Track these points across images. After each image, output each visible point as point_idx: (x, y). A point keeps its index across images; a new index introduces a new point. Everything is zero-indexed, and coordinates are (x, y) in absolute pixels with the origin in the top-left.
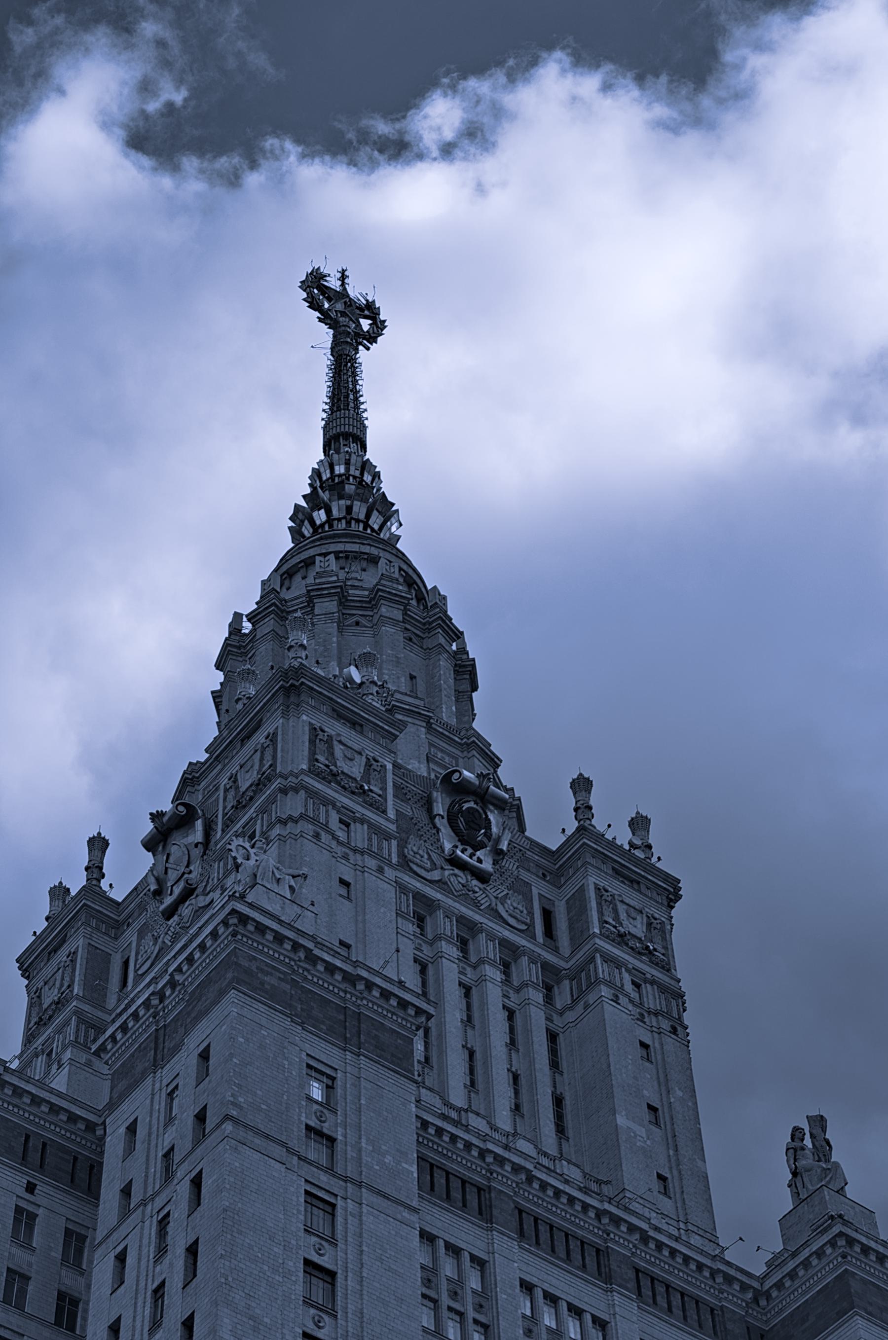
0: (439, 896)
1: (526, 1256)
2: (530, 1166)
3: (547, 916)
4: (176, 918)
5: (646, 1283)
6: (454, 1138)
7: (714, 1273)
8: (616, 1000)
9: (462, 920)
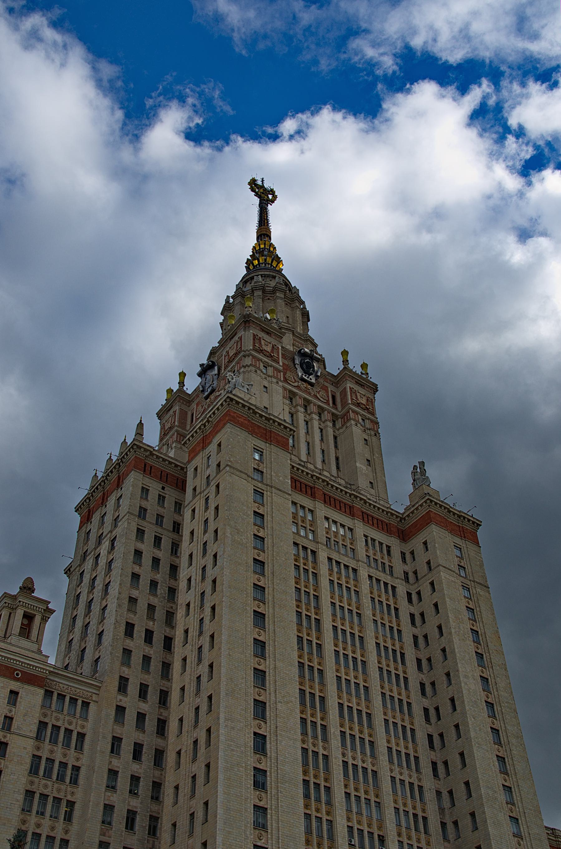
0: (297, 391)
1: (327, 508)
2: (328, 480)
3: (334, 397)
4: (209, 399)
5: (365, 516)
6: (303, 471)
7: (387, 512)
8: (356, 425)
9: (305, 399)
